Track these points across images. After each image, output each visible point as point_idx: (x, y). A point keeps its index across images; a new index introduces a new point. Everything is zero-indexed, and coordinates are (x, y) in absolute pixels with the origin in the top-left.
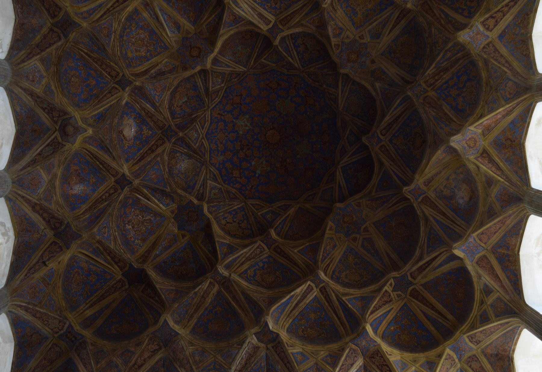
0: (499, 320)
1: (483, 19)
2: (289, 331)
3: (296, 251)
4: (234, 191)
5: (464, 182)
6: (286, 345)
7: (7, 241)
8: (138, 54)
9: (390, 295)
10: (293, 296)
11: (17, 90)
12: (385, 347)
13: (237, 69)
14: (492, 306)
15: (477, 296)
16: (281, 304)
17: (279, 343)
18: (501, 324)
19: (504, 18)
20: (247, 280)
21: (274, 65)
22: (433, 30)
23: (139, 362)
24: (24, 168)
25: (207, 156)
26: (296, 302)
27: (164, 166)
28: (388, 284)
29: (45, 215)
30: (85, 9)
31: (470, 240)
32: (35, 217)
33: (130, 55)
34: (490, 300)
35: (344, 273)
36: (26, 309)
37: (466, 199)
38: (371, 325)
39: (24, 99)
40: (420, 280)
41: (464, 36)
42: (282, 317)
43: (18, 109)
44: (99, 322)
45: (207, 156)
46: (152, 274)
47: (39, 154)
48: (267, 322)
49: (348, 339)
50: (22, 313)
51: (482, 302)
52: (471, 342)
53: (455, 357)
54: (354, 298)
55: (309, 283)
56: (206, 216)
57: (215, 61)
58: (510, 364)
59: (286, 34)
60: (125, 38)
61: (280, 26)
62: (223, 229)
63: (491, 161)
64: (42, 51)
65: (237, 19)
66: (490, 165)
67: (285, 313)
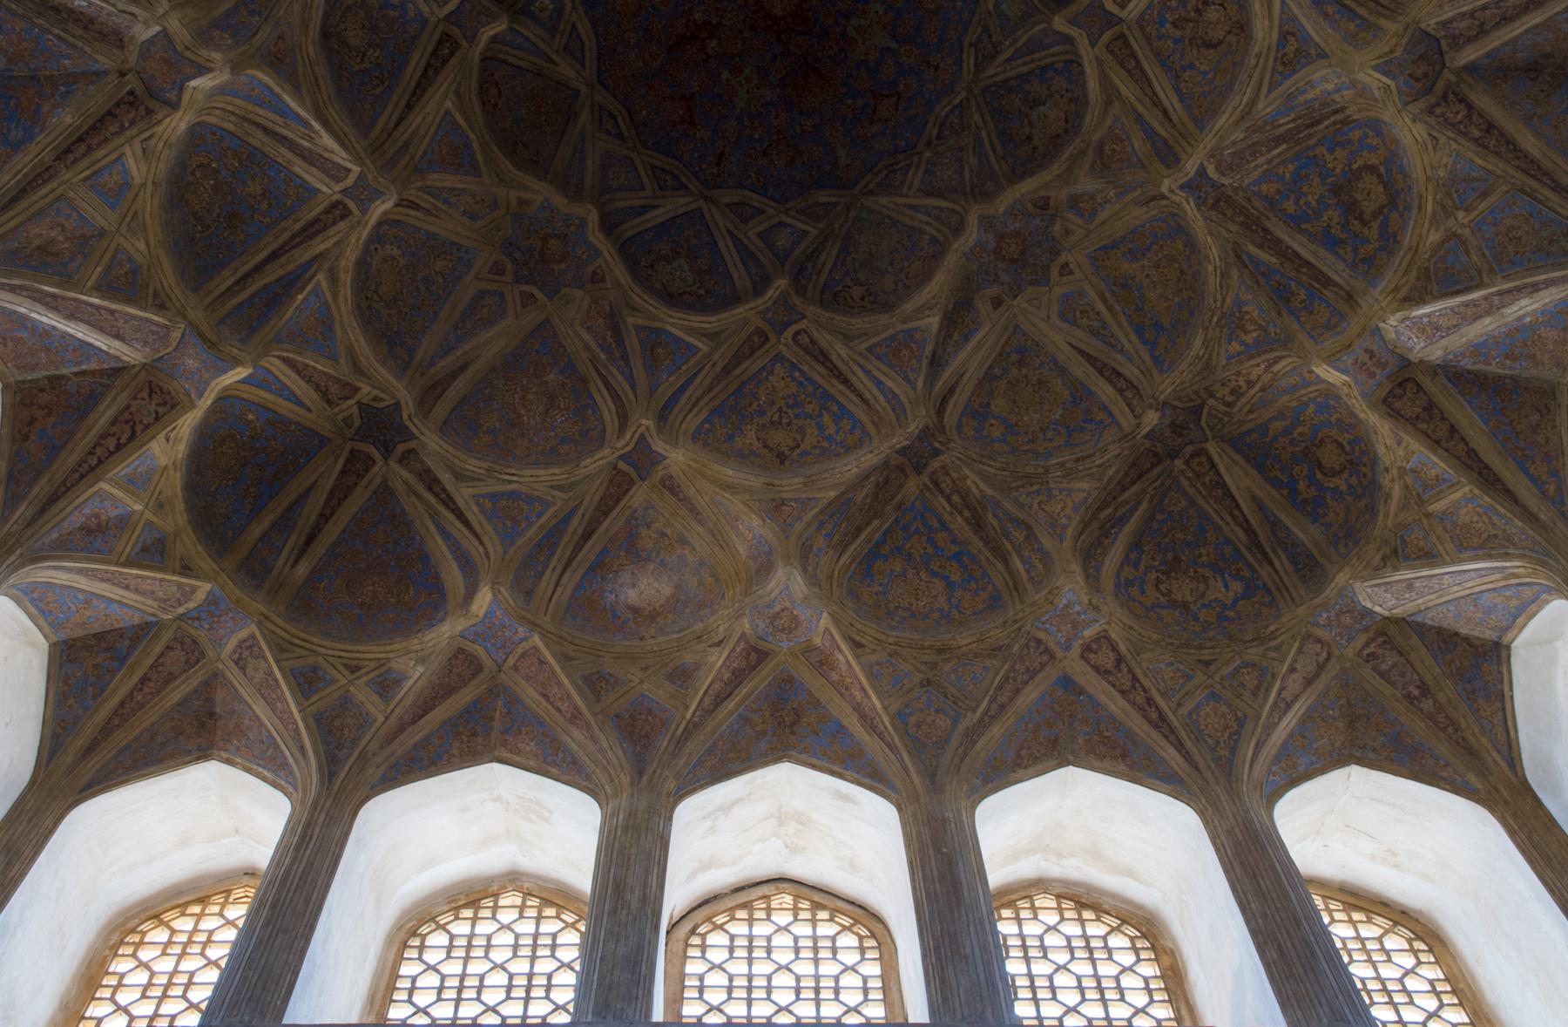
0: (308, 727)
1: (1114, 636)
3: (449, 104)
5: (676, 587)
6: (147, 134)
9: (346, 398)
10: (306, 124)
12: (187, 424)
14: (346, 701)
15: (370, 652)
16: (278, 96)
17: (149, 111)
18: (297, 731)
19: (1115, 693)
21: (991, 6)
22: (1085, 486)
26: (290, 135)
28: (376, 392)
31: (521, 629)
34: (363, 694)
35: (397, 252)
37: (632, 596)
38: (250, 375)
40: (401, 475)
41: (1071, 589)
42: (238, 102)
48: (210, 70)
49: (197, 315)
52: (239, 645)
53: (191, 605)
54: (326, 303)
55: (356, 169)
58: (189, 753)
59: (1083, 52)
61: (1107, 36)
63: (738, 677)
66: (727, 676)
67: (251, 107)
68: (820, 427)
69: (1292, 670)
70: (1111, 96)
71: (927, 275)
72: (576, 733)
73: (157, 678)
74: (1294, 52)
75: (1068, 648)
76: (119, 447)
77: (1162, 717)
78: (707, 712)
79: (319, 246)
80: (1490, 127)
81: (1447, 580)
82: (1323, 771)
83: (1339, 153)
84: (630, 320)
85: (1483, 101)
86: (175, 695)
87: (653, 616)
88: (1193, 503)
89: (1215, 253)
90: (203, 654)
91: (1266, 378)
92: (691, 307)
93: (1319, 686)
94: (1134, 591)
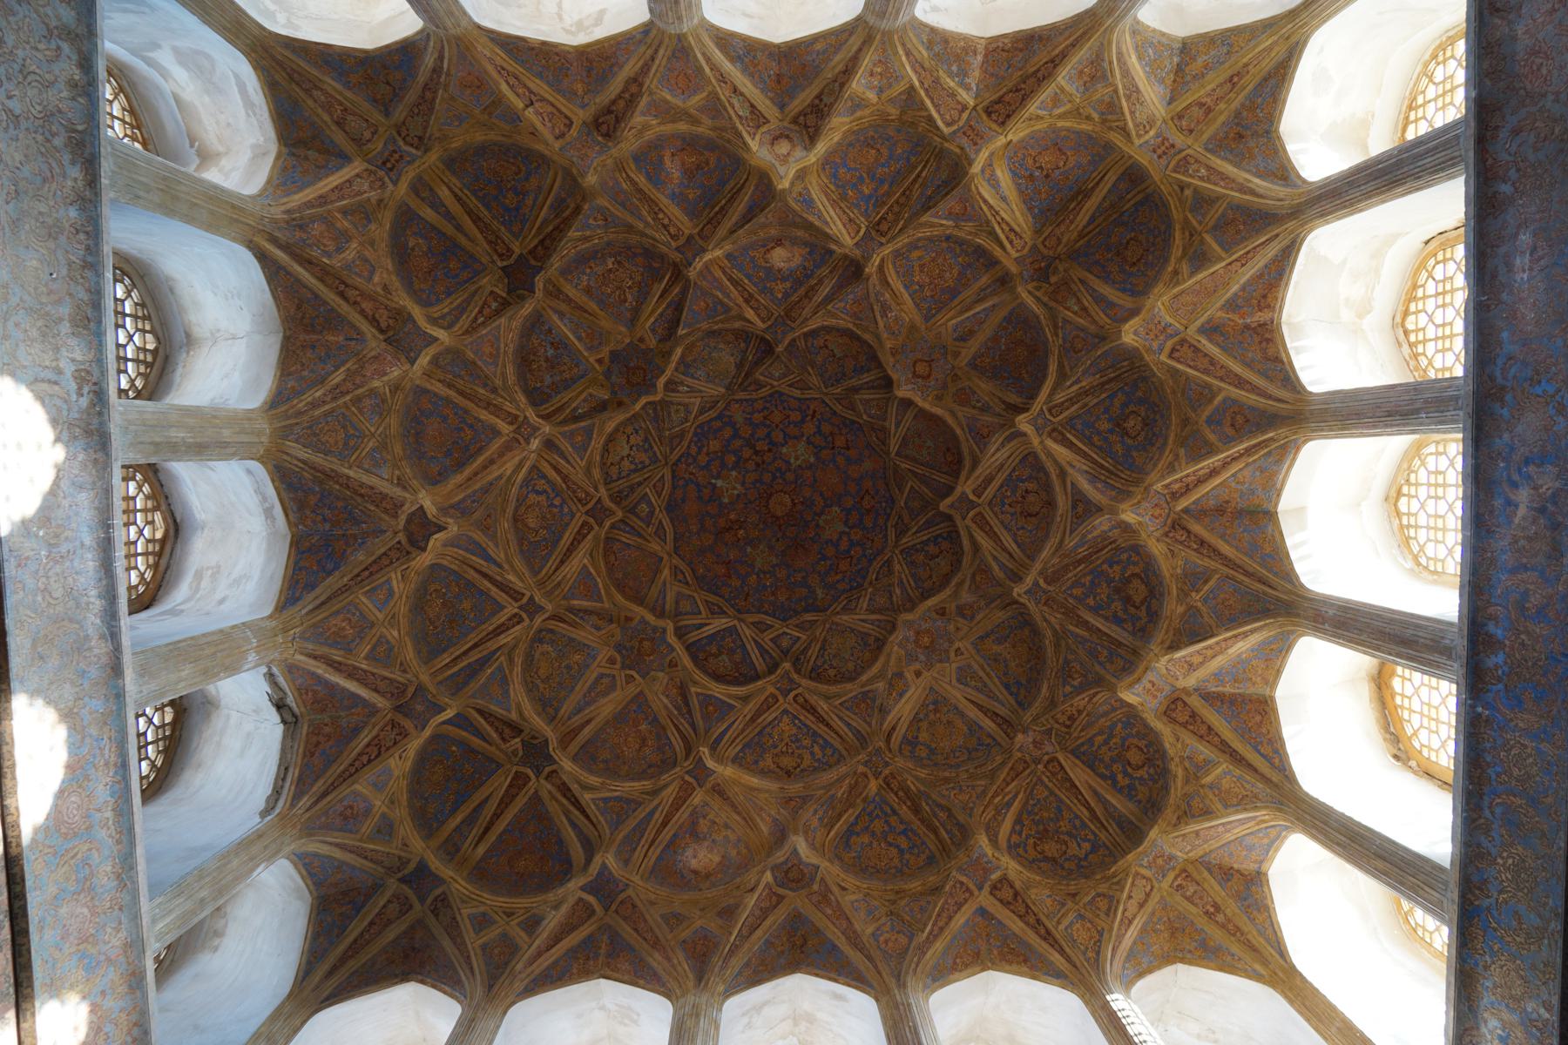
2: (433, 566)
4: (685, 443)
7: (568, 32)
8: (917, 269)
10: (500, 566)
11: (854, 43)
12: (414, 745)
13: (893, 442)
15: (521, 903)
20: (527, 482)
23: (351, 293)
24: (708, 60)
25: (742, 395)
27: (722, 322)
29: (622, 103)
30: (999, 173)
32: (615, 86)
33: (915, 254)
36: (437, 70)
37: (694, 864)
38: (458, 715)
39: (838, 58)
40: (546, 787)
43: (818, 46)
44: (428, 213)
45: (742, 395)
46: (527, 309)
47: (735, 90)
50: (429, 60)
51: (509, 915)
52: (436, 899)
53: (406, 872)
56: (637, 400)
57: (907, 403)
58: (396, 976)
60: (945, 245)
61: (971, 514)
62: (616, 430)
63: (765, 913)
64: (926, 90)
65: (982, 438)
66: (757, 913)
68: (812, 753)
69: (1130, 897)
70: (976, 547)
71: (874, 660)
72: (656, 955)
73: (381, 922)
74: (1083, 508)
75: (980, 888)
76: (370, 761)
77: (1048, 932)
78: (744, 937)
79: (503, 639)
80: (1202, 543)
81: (1221, 829)
82: (1159, 967)
83: (1116, 567)
84: (693, 689)
85: (1196, 528)
86: (391, 934)
87: (708, 876)
88: (1052, 793)
89: (1049, 633)
90: (411, 907)
91: (1089, 707)
92: (729, 683)
93: (1149, 908)
94: (1021, 851)
